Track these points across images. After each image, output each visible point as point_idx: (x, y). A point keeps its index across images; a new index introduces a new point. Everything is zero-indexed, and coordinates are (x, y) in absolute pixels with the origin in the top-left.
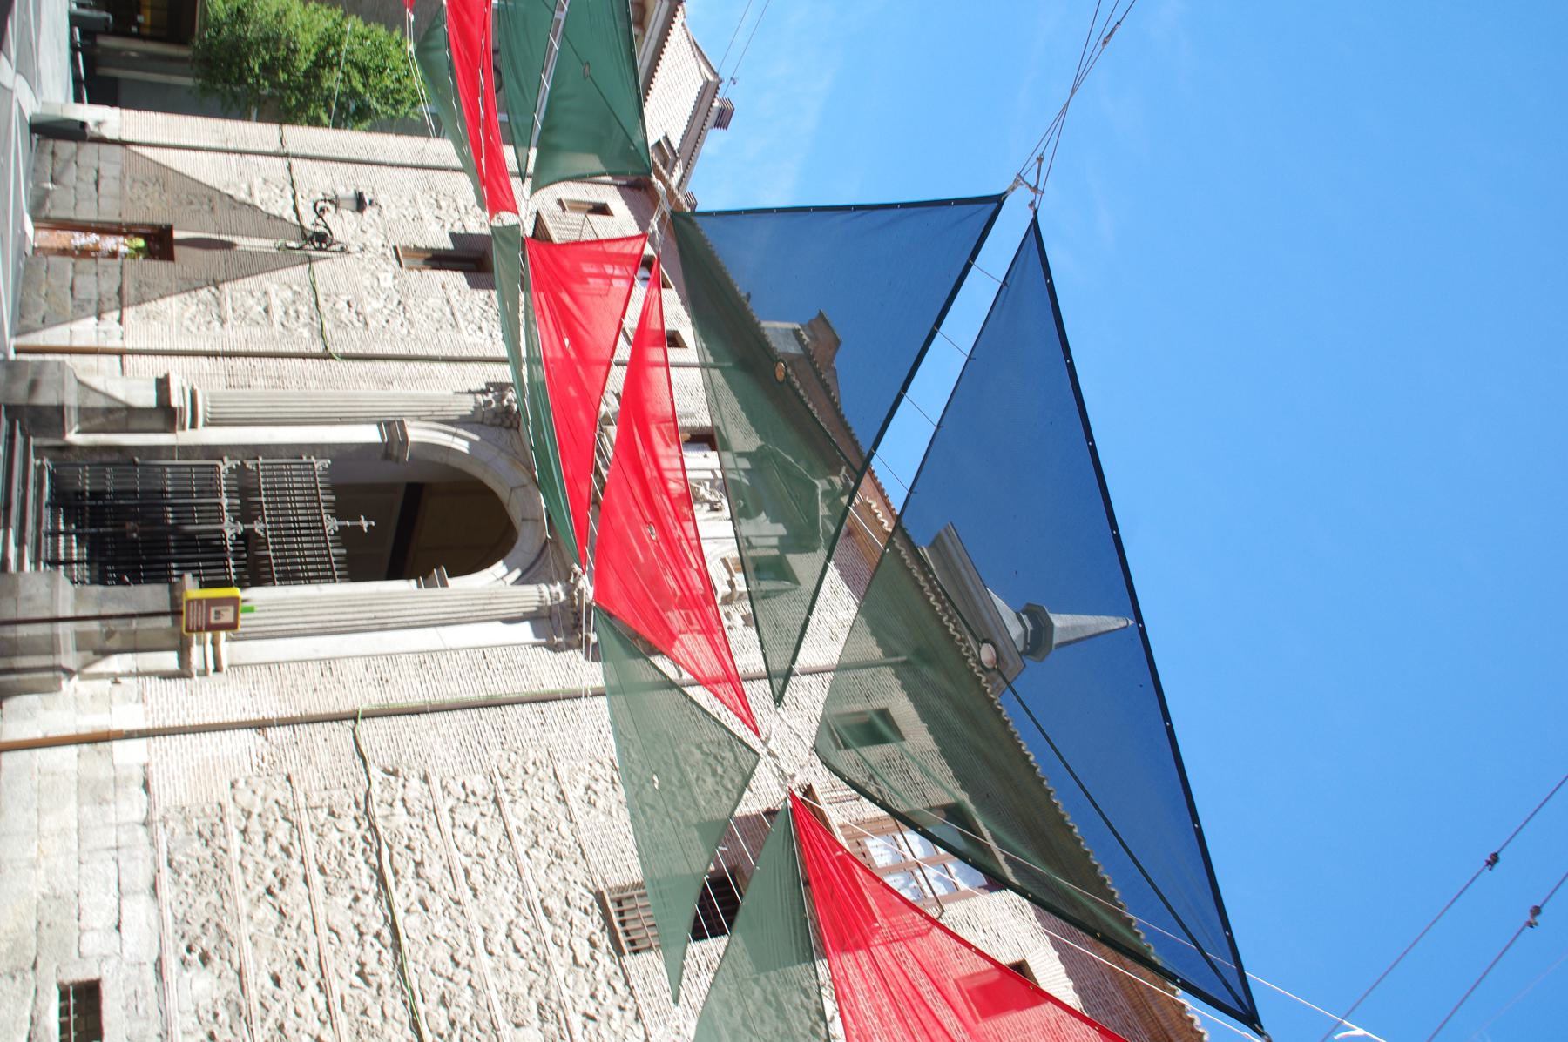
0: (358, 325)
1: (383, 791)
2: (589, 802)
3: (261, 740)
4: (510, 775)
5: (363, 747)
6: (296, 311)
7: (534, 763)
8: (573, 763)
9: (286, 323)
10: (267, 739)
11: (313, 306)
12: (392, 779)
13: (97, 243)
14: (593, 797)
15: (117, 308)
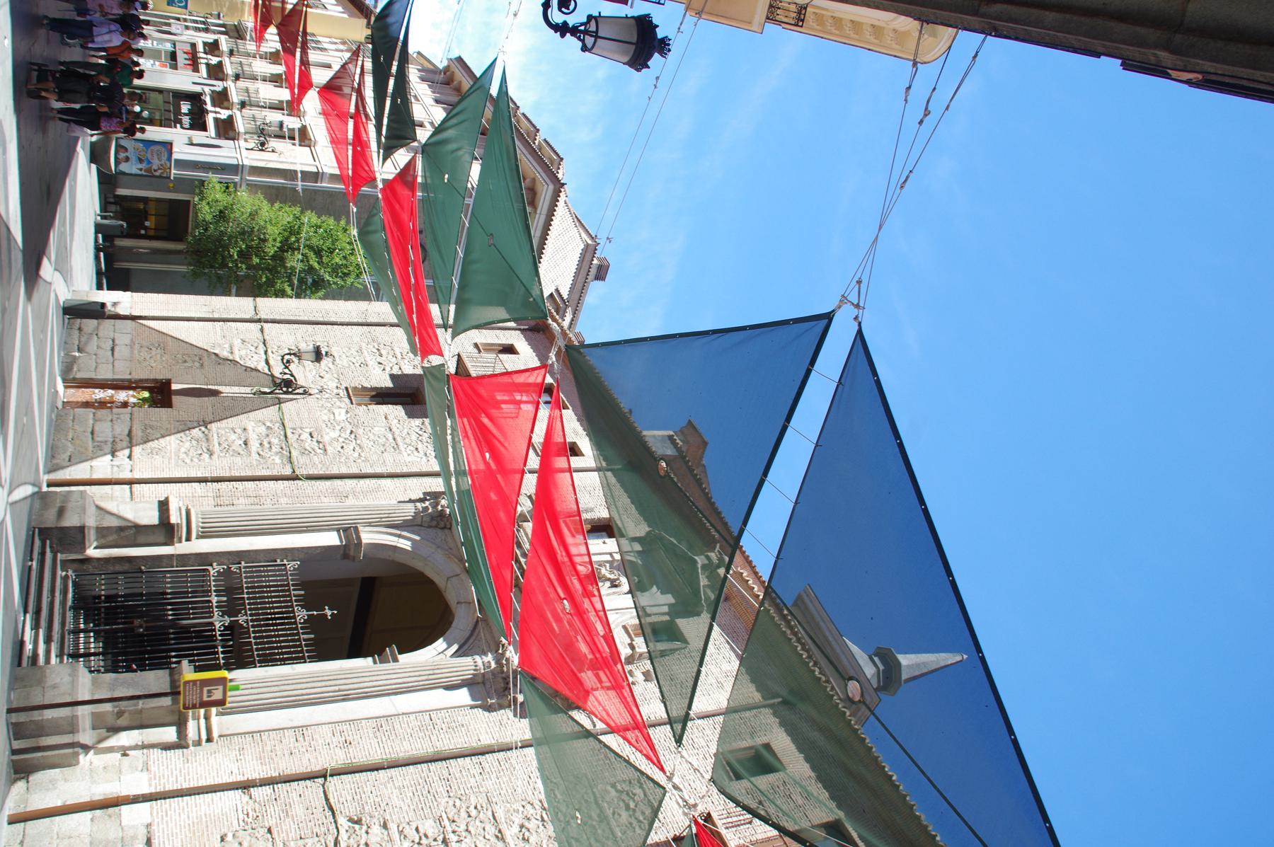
0: (319, 451)
1: (349, 838)
2: (524, 839)
3: (246, 798)
4: (455, 819)
5: (332, 801)
6: (269, 443)
7: (476, 808)
8: (508, 805)
9: (261, 453)
10: (251, 798)
11: (283, 438)
12: (357, 827)
14: (527, 834)
15: (128, 448)
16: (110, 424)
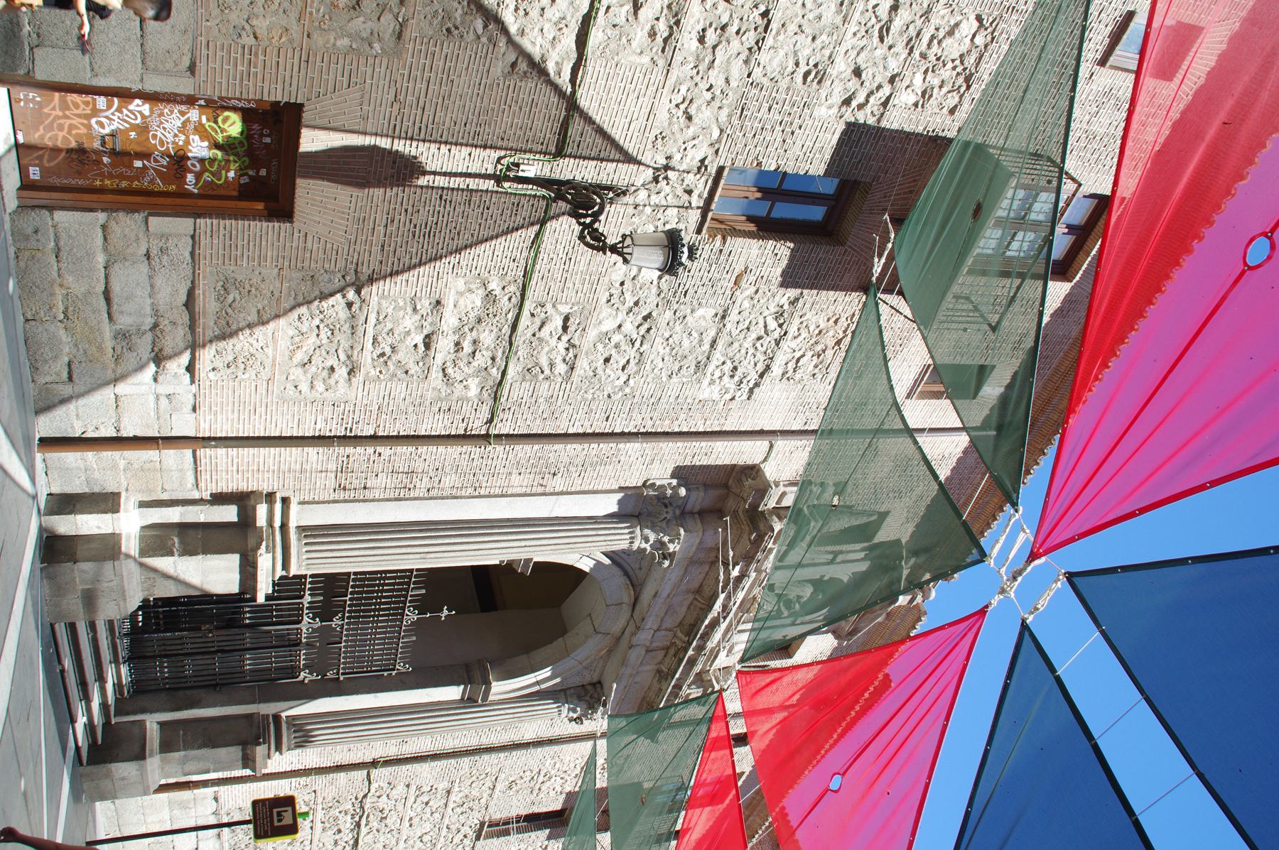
9: (450, 371)
11: (506, 330)
13: (144, 129)
16: (144, 268)
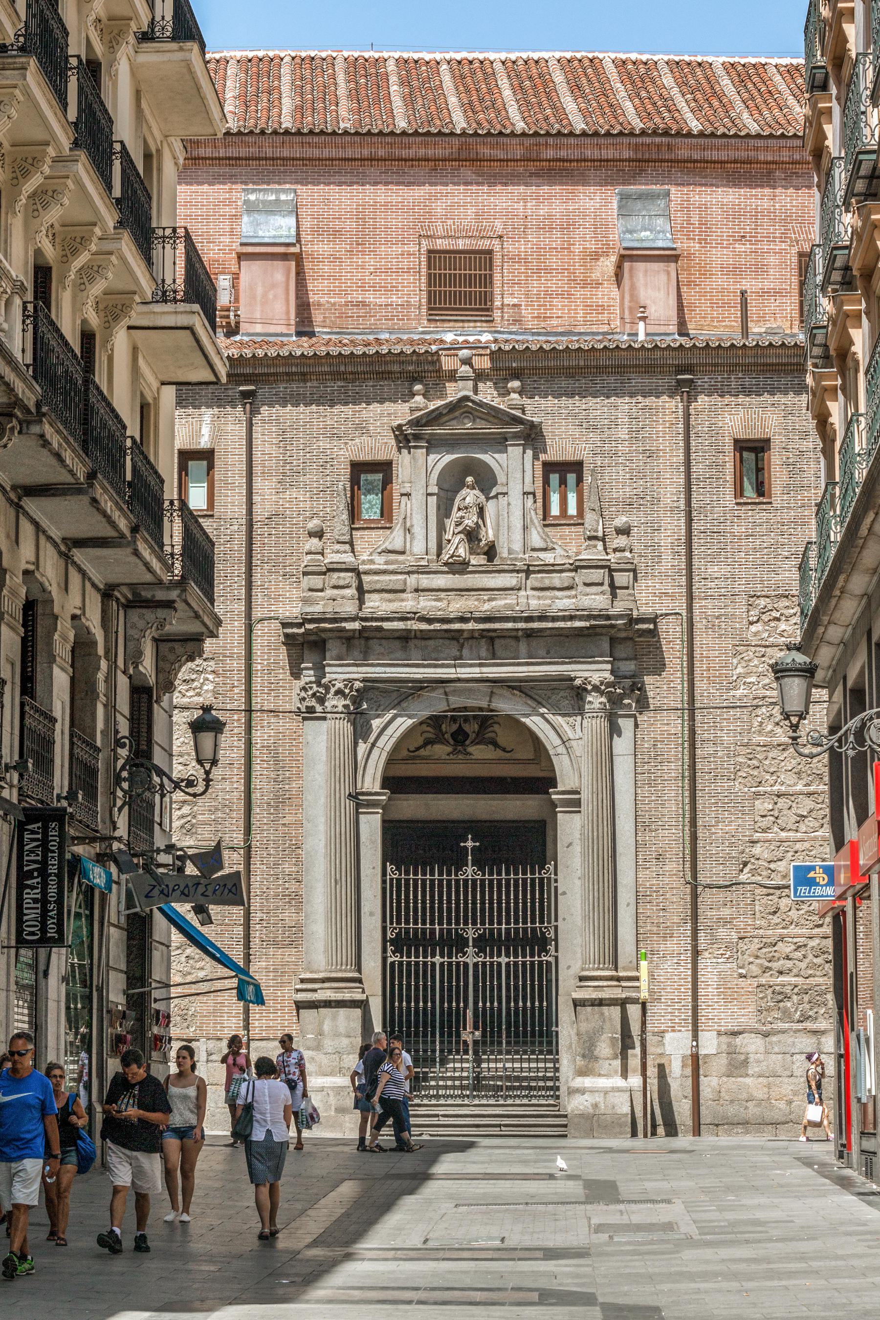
12: (749, 866)
